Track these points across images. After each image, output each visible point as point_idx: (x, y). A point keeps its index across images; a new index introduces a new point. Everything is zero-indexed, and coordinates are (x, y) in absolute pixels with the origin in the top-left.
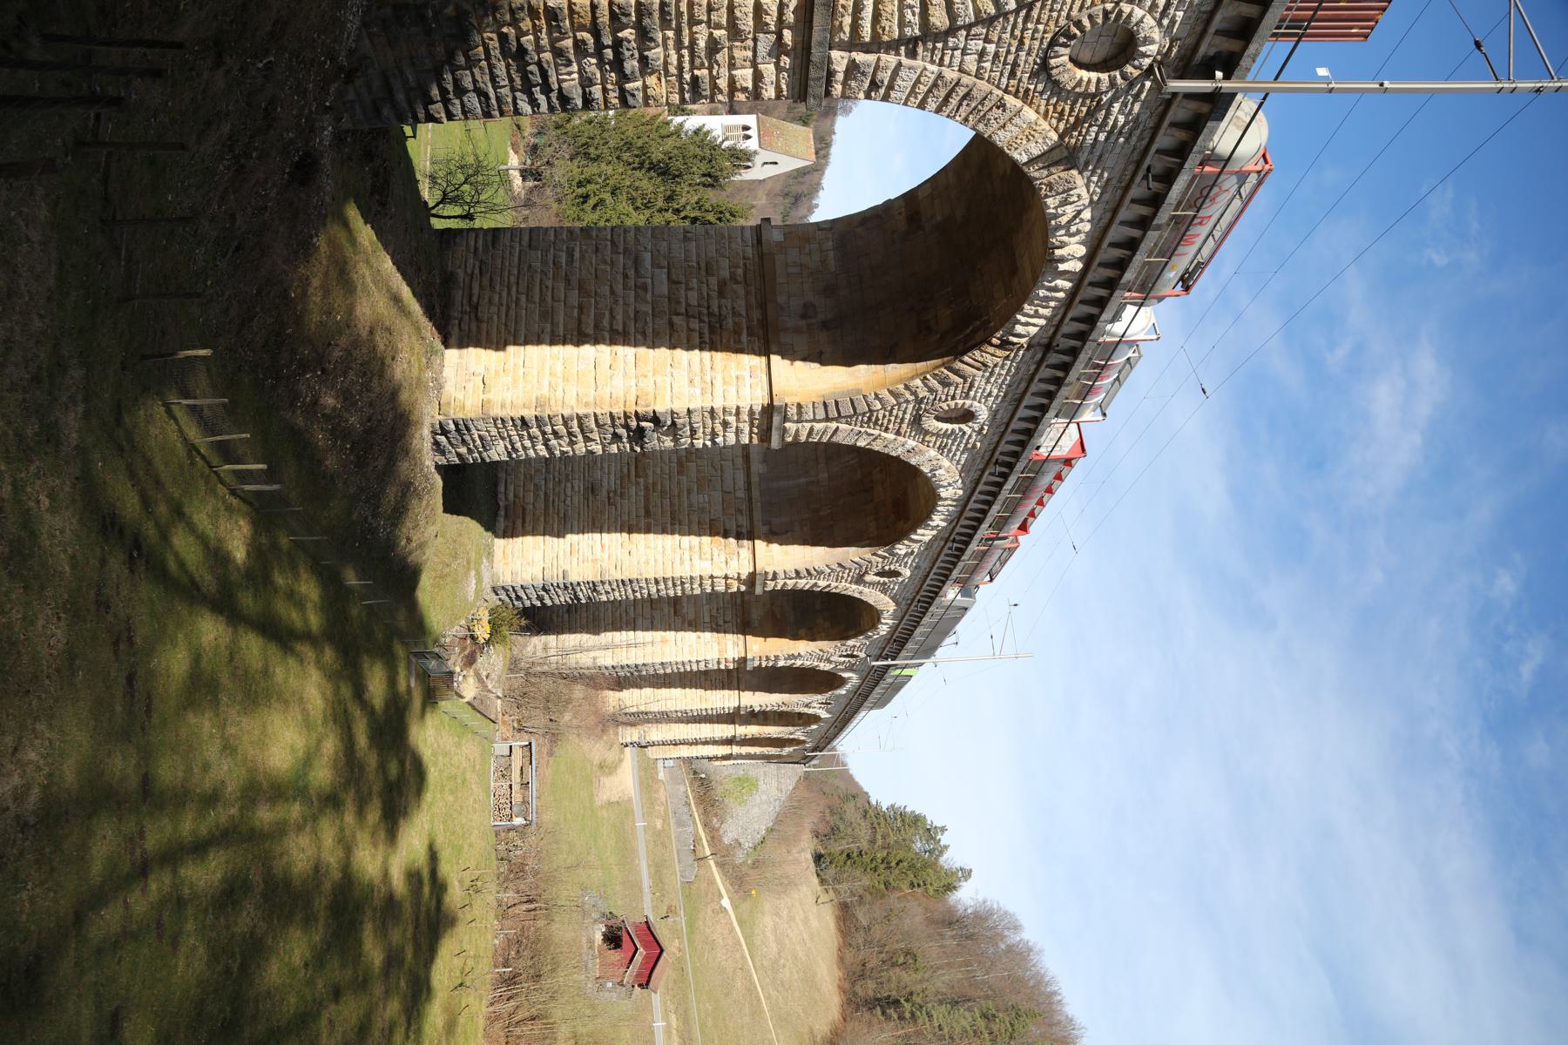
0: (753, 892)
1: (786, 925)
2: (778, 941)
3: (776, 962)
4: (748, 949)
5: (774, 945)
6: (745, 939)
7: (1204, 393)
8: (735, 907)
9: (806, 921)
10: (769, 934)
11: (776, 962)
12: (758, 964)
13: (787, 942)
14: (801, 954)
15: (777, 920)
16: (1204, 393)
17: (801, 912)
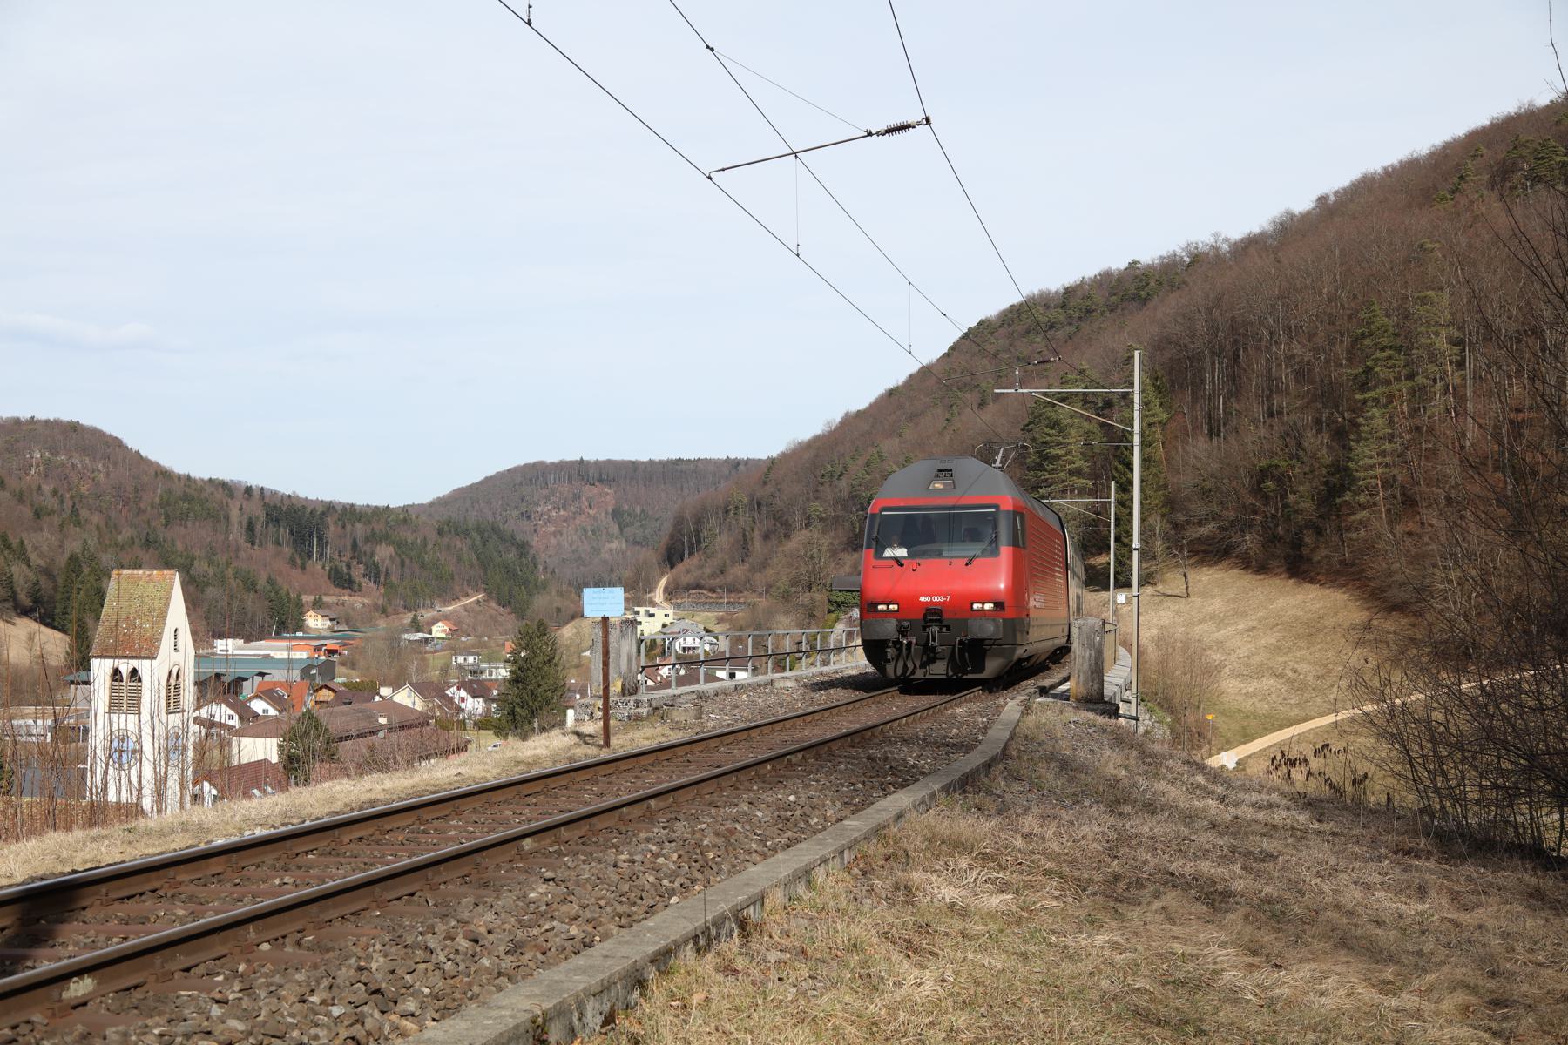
0: (1210, 717)
1: (1233, 657)
2: (1258, 674)
3: (1290, 682)
4: (1281, 727)
5: (1264, 679)
6: (1268, 730)
7: (904, 127)
8: (1227, 745)
9: (1219, 620)
10: (1251, 689)
11: (1290, 682)
12: (1297, 711)
13: (1256, 659)
14: (1271, 639)
15: (1227, 670)
16: (904, 127)
17: (1205, 626)
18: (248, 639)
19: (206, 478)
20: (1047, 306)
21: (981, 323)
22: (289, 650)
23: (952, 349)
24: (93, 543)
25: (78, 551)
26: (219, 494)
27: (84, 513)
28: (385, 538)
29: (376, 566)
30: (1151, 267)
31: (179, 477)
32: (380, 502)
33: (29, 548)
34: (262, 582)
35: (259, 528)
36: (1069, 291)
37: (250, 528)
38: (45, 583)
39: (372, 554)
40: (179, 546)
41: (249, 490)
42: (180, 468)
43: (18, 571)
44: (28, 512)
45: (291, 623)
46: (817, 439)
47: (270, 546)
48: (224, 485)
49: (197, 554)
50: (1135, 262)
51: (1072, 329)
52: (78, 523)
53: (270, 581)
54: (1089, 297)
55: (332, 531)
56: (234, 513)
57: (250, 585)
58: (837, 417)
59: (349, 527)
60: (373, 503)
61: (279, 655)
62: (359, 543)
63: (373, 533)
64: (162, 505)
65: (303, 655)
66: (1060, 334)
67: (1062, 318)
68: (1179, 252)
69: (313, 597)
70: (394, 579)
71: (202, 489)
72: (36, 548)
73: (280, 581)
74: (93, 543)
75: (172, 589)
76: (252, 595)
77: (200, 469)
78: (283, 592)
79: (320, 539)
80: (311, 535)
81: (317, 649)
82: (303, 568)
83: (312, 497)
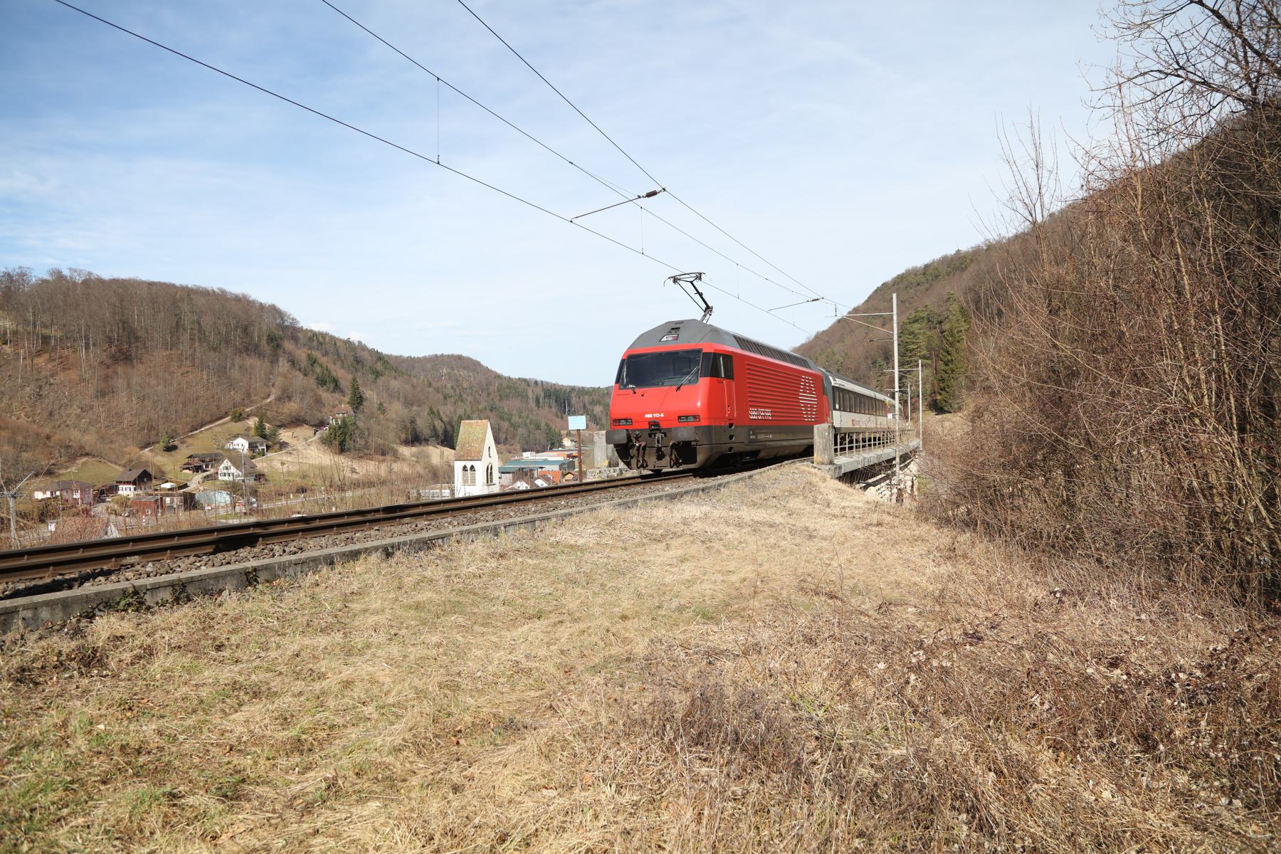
18: (538, 452)
19: (517, 377)
20: (916, 274)
21: (883, 285)
22: (558, 455)
23: (869, 298)
24: (468, 410)
25: (462, 414)
26: (523, 385)
27: (464, 396)
28: (599, 403)
29: (595, 416)
30: (967, 252)
31: (505, 378)
32: (597, 386)
33: (441, 413)
34: (543, 425)
35: (541, 401)
36: (927, 267)
37: (537, 400)
38: (448, 427)
39: (593, 410)
40: (506, 410)
41: (536, 382)
42: (505, 374)
43: (438, 424)
44: (441, 396)
45: (557, 444)
46: (803, 345)
47: (547, 408)
48: (525, 380)
49: (514, 412)
50: (959, 251)
51: (927, 285)
52: (462, 401)
53: (547, 425)
54: (937, 270)
55: (574, 400)
56: (530, 394)
57: (538, 428)
58: (813, 334)
59: (581, 398)
60: (593, 386)
61: (550, 459)
62: (589, 407)
63: (593, 401)
64: (498, 391)
65: (561, 459)
66: (922, 288)
67: (923, 280)
68: (981, 244)
69: (565, 432)
70: (604, 421)
71: (516, 383)
72: (444, 413)
73: (551, 424)
74: (468, 410)
75: (486, 431)
76: (538, 431)
77: (515, 374)
78: (552, 429)
79: (569, 404)
80: (564, 403)
81: (569, 456)
82: (562, 418)
83: (565, 384)
